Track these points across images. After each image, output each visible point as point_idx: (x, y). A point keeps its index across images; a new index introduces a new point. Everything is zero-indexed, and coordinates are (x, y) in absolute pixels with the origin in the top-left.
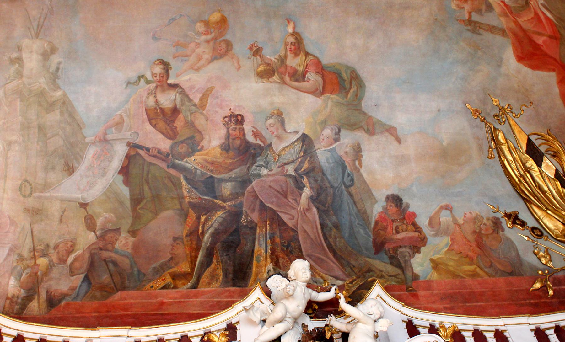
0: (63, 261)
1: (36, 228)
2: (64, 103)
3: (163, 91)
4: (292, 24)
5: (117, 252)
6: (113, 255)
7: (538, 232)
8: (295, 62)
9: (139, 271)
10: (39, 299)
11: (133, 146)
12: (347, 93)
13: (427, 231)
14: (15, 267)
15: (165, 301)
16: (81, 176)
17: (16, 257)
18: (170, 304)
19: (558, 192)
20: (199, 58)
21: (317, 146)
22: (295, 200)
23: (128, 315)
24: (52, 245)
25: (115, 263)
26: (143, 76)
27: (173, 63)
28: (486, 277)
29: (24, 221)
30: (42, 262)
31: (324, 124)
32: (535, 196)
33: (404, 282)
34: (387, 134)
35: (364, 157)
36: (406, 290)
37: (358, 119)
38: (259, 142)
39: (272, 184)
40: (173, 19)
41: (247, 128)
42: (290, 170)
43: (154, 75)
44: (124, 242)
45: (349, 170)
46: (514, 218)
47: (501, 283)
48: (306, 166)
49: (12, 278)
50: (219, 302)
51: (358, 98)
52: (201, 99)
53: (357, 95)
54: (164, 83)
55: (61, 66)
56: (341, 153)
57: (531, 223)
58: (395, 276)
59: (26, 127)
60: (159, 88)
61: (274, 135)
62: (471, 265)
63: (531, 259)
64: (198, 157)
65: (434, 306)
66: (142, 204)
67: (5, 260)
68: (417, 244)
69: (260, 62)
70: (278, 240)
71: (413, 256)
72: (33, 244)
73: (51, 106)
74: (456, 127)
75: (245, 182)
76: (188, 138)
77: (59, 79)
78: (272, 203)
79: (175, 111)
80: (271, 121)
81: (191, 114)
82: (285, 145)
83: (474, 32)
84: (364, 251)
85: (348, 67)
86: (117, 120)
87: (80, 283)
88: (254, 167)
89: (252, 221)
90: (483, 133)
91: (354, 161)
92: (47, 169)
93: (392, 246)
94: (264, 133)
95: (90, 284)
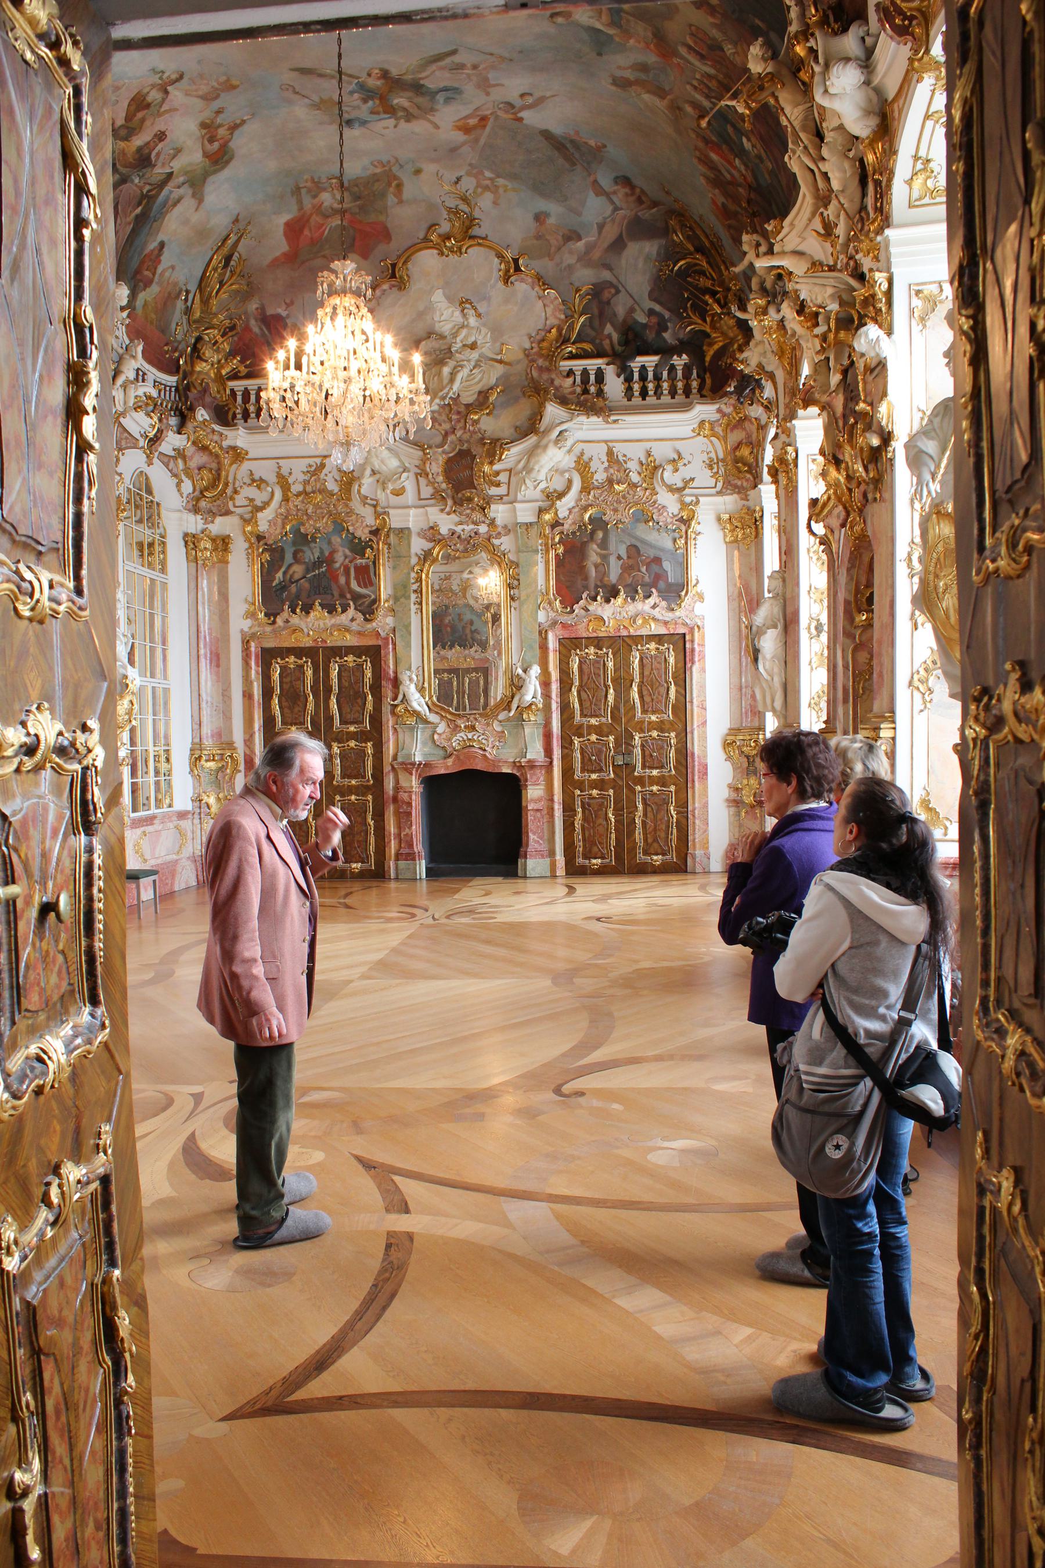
8: (221, 132)
51: (215, 172)
79: (148, 106)
90: (225, 233)
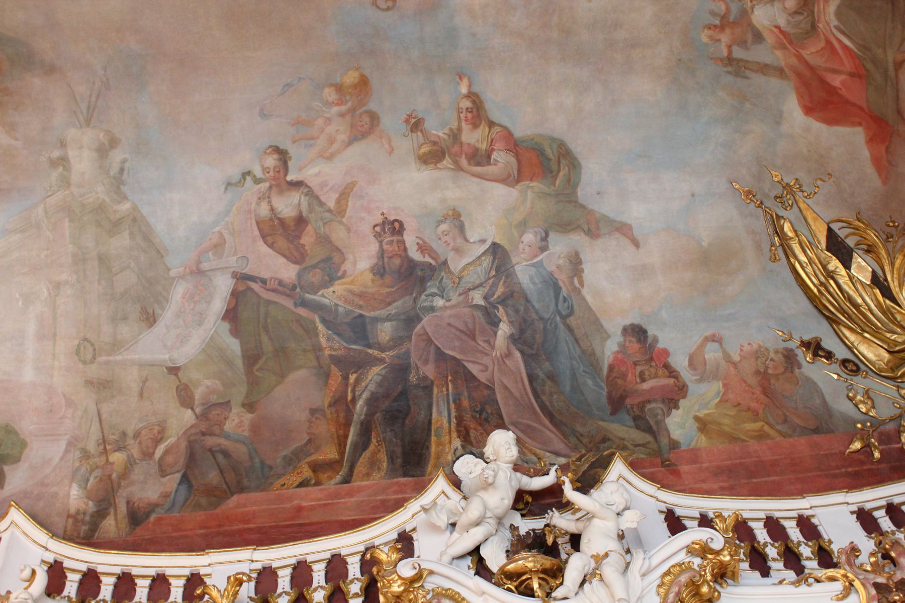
0: (148, 455)
1: (105, 408)
2: (135, 220)
3: (281, 192)
4: (465, 81)
5: (227, 437)
6: (222, 441)
7: (852, 366)
8: (473, 137)
9: (262, 463)
10: (116, 515)
11: (242, 278)
12: (555, 178)
13: (687, 375)
14: (78, 469)
15: (304, 504)
16: (167, 327)
17: (78, 454)
18: (312, 508)
19: (879, 305)
20: (332, 141)
21: (514, 260)
22: (488, 342)
23: (250, 529)
24: (130, 433)
25: (226, 454)
26: (249, 173)
27: (292, 150)
28: (779, 438)
29: (87, 400)
30: (118, 458)
31: (523, 226)
32: (844, 312)
33: (658, 453)
34: (617, 235)
35: (586, 271)
36: (661, 465)
37: (572, 215)
38: (428, 259)
39: (452, 321)
40: (289, 85)
41: (410, 239)
42: (477, 298)
43: (265, 170)
44: (237, 422)
45: (564, 292)
46: (815, 348)
47: (802, 445)
48: (500, 290)
49: (74, 485)
50: (383, 502)
51: (572, 183)
52: (338, 201)
53: (569, 181)
54: (282, 180)
55: (127, 165)
56: (551, 267)
57: (841, 353)
58: (643, 445)
59: (80, 260)
60: (274, 190)
61: (450, 248)
62: (755, 421)
63: (843, 406)
64: (338, 288)
65: (705, 486)
66: (261, 362)
67: (62, 459)
68: (673, 397)
69: (421, 140)
70: (466, 403)
71: (669, 414)
72: (103, 432)
73: (115, 226)
74: (720, 217)
75: (410, 320)
76: (323, 261)
77: (124, 185)
78: (453, 349)
79: (301, 221)
80: (444, 227)
81: (325, 224)
82: (467, 261)
83: (737, 74)
84: (595, 413)
85: (553, 139)
86: (215, 240)
87: (175, 486)
88: (423, 297)
89: (425, 378)
90: (761, 224)
91: (572, 278)
92: (118, 318)
93: (636, 402)
94: (434, 245)
95: (190, 486)
